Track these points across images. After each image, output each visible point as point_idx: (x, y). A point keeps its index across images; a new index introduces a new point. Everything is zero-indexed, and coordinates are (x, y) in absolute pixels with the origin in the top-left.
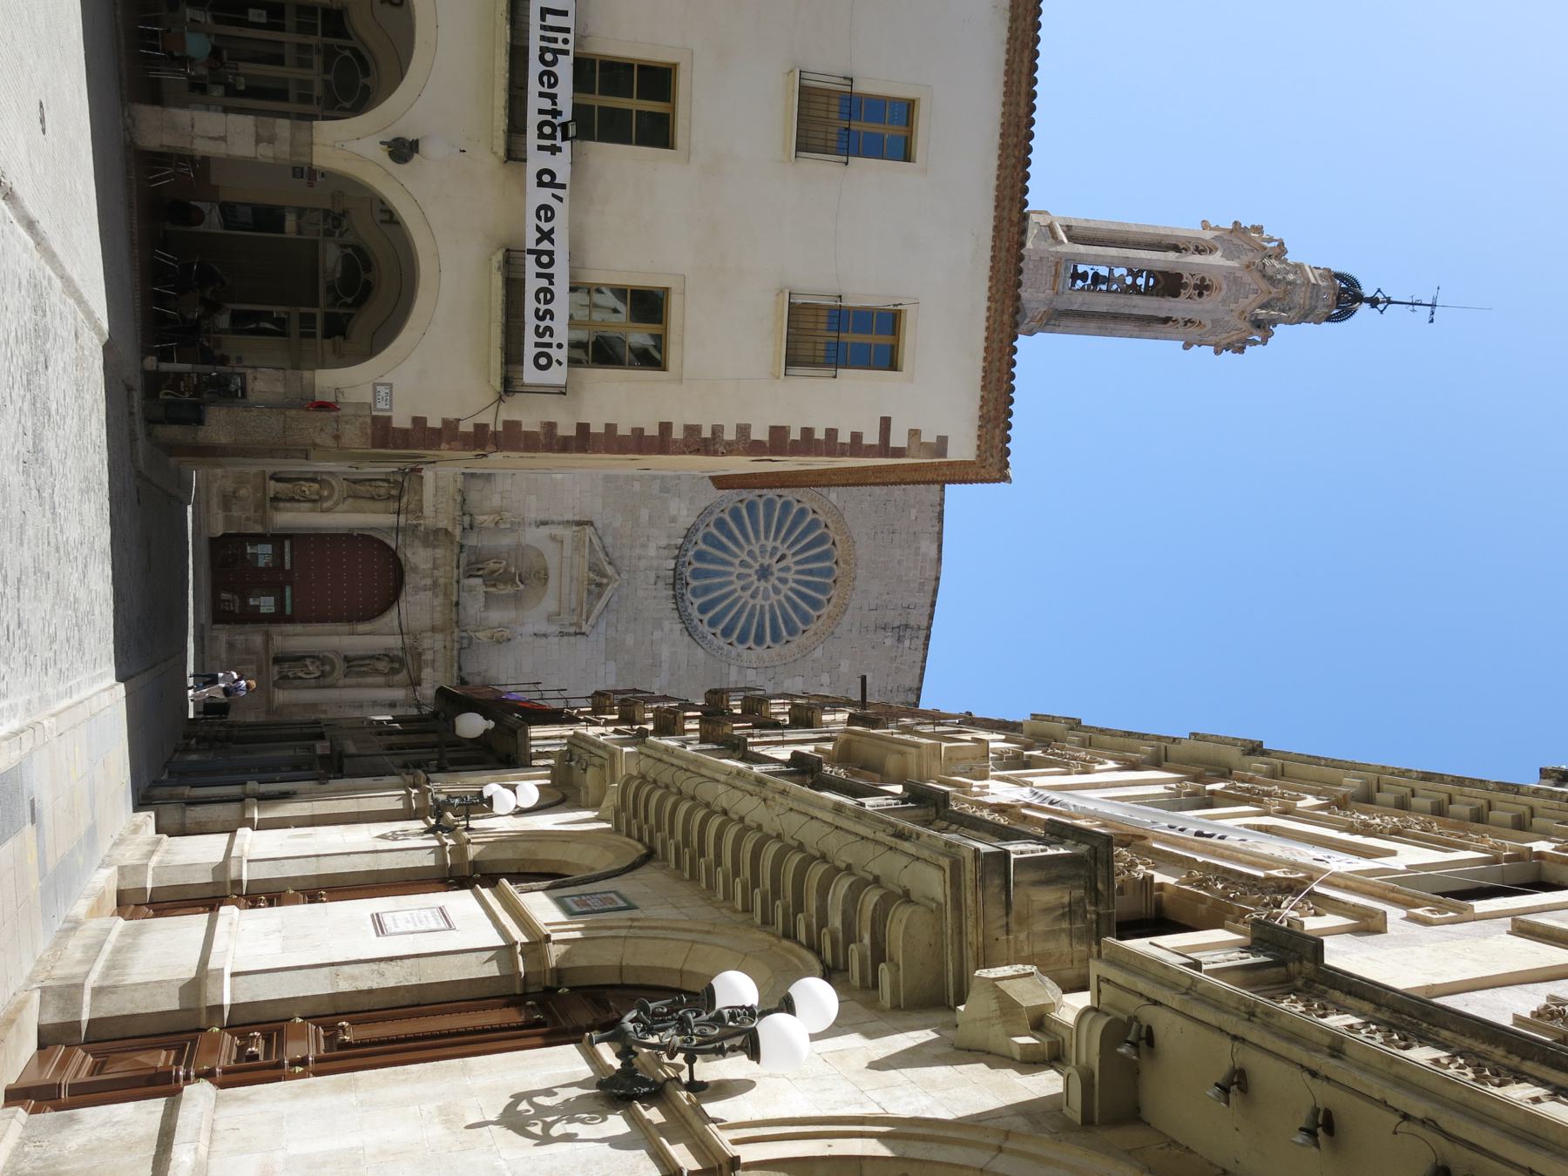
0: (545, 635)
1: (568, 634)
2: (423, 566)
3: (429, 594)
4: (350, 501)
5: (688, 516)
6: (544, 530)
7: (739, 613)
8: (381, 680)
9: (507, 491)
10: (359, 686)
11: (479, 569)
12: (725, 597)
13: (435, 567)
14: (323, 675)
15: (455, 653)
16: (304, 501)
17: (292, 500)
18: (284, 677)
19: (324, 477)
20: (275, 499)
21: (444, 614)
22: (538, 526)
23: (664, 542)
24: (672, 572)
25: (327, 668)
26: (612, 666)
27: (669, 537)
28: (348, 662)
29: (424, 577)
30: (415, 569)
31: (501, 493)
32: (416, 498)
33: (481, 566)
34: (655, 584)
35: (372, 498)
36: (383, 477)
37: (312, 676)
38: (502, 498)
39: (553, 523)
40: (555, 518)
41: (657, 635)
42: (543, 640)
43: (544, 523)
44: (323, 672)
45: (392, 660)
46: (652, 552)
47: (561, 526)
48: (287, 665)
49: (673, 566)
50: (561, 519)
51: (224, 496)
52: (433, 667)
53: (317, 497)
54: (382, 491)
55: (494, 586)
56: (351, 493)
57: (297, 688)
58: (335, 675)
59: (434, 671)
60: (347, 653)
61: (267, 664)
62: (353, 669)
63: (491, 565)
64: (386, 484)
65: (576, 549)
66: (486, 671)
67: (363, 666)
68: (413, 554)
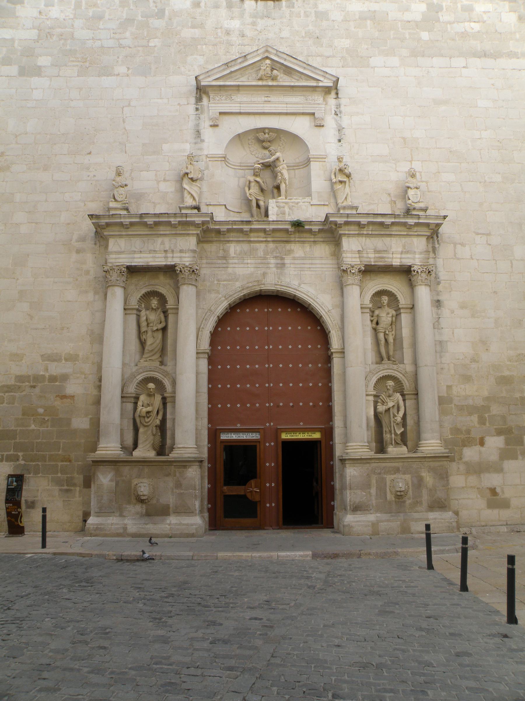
0: (340, 130)
1: (338, 106)
6: (207, 133)
8: (405, 318)
9: (156, 175)
10: (414, 345)
11: (258, 206)
14: (400, 388)
16: (165, 415)
17: (162, 427)
18: (403, 439)
20: (161, 450)
22: (203, 141)
26: (377, 61)
33: (254, 204)
35: (164, 330)
37: (401, 403)
38: (165, 180)
39: (198, 125)
40: (191, 124)
41: (336, 16)
43: (198, 133)
46: (235, 24)
48: (387, 437)
50: (192, 118)
51: (148, 514)
53: (158, 399)
55: (278, 188)
56: (158, 355)
62: (391, 353)
64: (143, 313)
66: (389, 194)
67: (386, 340)
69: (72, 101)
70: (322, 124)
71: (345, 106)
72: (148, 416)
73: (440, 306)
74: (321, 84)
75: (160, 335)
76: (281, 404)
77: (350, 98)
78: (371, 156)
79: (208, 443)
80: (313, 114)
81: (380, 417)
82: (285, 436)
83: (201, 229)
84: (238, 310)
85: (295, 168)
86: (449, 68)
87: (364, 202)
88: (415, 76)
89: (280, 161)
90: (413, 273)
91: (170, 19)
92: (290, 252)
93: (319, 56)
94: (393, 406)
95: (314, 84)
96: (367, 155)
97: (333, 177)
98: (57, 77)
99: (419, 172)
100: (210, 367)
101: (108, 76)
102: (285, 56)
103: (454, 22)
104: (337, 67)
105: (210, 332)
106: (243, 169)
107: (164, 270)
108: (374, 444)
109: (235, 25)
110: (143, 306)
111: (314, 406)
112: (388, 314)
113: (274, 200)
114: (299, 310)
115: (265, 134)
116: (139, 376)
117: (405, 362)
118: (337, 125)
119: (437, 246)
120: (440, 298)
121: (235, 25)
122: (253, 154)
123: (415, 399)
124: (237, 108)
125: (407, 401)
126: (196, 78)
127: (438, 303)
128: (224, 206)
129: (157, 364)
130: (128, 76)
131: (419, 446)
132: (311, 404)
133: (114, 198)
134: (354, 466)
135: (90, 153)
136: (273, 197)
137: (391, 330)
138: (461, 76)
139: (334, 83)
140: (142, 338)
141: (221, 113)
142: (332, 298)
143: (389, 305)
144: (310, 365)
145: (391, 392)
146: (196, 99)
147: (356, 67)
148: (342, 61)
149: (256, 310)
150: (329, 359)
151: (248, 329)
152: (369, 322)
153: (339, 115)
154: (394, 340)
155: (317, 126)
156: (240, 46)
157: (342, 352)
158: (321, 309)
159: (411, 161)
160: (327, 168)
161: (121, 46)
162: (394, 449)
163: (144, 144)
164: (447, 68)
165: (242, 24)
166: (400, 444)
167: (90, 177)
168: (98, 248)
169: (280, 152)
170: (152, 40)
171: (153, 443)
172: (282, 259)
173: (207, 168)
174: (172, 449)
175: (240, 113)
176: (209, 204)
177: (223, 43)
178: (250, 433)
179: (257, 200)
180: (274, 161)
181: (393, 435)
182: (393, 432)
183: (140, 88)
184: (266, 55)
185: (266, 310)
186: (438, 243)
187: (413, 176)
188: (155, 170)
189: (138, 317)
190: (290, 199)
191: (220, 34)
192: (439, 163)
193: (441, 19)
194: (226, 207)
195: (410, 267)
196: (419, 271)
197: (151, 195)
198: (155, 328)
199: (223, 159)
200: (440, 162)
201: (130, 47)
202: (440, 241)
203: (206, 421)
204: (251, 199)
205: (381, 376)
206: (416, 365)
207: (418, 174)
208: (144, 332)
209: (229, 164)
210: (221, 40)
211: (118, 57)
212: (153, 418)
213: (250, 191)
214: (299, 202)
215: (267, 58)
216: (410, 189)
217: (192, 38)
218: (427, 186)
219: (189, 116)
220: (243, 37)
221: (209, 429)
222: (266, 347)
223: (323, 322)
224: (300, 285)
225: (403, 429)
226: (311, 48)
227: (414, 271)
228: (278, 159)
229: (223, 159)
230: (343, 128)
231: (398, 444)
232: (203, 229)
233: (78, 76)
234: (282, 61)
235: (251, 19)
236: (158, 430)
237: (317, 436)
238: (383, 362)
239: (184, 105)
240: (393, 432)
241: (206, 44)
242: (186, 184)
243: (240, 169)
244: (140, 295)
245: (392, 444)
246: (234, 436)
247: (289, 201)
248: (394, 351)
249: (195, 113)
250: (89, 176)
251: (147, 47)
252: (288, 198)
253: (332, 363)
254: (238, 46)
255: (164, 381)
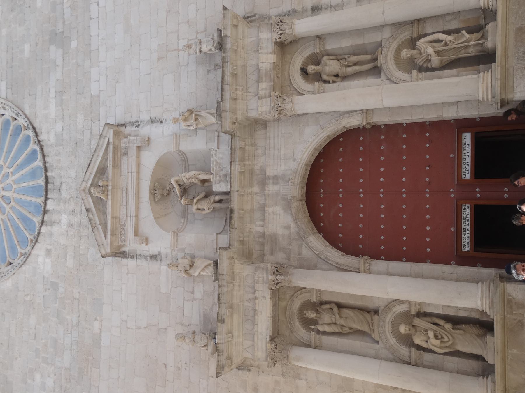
0: (152, 121)
1: (132, 124)
2: (279, 209)
3: (269, 172)
4: (371, 305)
5: (38, 256)
6: (152, 249)
7: (9, 152)
8: (331, 46)
9: (187, 300)
10: (360, 32)
11: (220, 201)
12: (21, 167)
13: (262, 208)
14: (412, 43)
15: (228, 95)
19: (404, 351)
21: (254, 145)
22: (159, 254)
23: (56, 229)
24: (49, 196)
25: (405, 53)
27: (51, 234)
28: (376, 67)
29: (277, 194)
30: (287, 205)
31: (194, 299)
32: (283, 304)
33: (217, 205)
34: (61, 183)
35: (340, 306)
36: (324, 338)
38: (193, 292)
39: (146, 257)
40: (144, 263)
42: (153, 116)
43: (153, 257)
44: (414, 47)
45: (318, 77)
47: (139, 253)
48: (472, 52)
49: (49, 202)
50: (139, 261)
52: (259, 70)
53: (417, 322)
54: (326, 318)
55: (204, 181)
56: (368, 316)
57: (455, 14)
58: (395, 44)
59: (258, 65)
60: (377, 81)
61: (506, 49)
62: (369, 57)
63: (205, 205)
64: (321, 328)
65: (123, 226)
67: (355, 64)
68: (288, 227)
69: (119, 377)
70: (147, 139)
71: (131, 117)
72: (440, 337)
73: (318, 7)
74: (111, 140)
75: (345, 311)
76: (427, 179)
77: (125, 113)
78: (174, 91)
79: (477, 266)
80: (139, 147)
81: (447, 63)
82: (467, 175)
83: (236, 260)
84: (322, 224)
85: (187, 165)
86: (99, 19)
87: (216, 96)
88: (106, 51)
89: (179, 180)
90: (283, 39)
91: (59, 277)
92: (263, 171)
93: (90, 142)
94: (433, 47)
95: (111, 147)
96: (173, 95)
97: (192, 128)
98: (99, 389)
99: (188, 42)
100: (382, 258)
101: (101, 340)
102: (88, 173)
103: (64, 18)
104: (100, 125)
105: (342, 255)
106: (188, 216)
107: (277, 301)
108: (482, 66)
109: (66, 218)
110: (313, 327)
111: (430, 141)
112: (326, 65)
113: (214, 185)
114: (322, 161)
115: (156, 193)
116: (391, 340)
117: (379, 40)
118: (148, 125)
119: (257, 17)
120: (310, 7)
121: (66, 218)
122: (174, 205)
123: (425, 22)
124: (132, 219)
125: (427, 32)
126: (103, 257)
127: (316, 9)
128: (219, 235)
129: (376, 317)
130: (101, 321)
131: (487, 8)
132: (428, 145)
133: (205, 346)
134: (513, 87)
135: (165, 365)
136: (211, 186)
137: (344, 59)
138: (105, 7)
139: (110, 128)
140: (348, 332)
141: (136, 235)
142: (308, 125)
143: (317, 63)
144: (382, 148)
145: (415, 52)
146: (123, 258)
147: (100, 108)
148: (94, 121)
149: (322, 205)
150: (376, 128)
151: (341, 215)
152: (335, 84)
153: (139, 123)
154: (354, 55)
155: (149, 144)
156: (82, 215)
157: (367, 112)
158: (319, 137)
159: (179, 51)
160: (185, 134)
161: (78, 325)
162: (489, 39)
163: (160, 311)
164: (99, 21)
165: (65, 212)
166: (484, 33)
167: (186, 367)
168: (254, 368)
169: (170, 179)
170: (74, 296)
171: (476, 335)
172: (269, 178)
173: (183, 250)
174: (483, 313)
175: (137, 217)
176: (215, 250)
177: (79, 230)
178: (463, 216)
179: (215, 202)
180: (180, 186)
181: (471, 43)
182: (465, 44)
183: (112, 310)
184: (87, 191)
185: (322, 195)
186: (254, 16)
187: (189, 47)
188: (184, 302)
189: (325, 333)
190: (213, 169)
191: (72, 233)
192: (180, 22)
193: (61, 30)
194: (220, 233)
195: (276, 43)
196: (281, 32)
197: (205, 307)
198: (337, 316)
199: (176, 234)
200: (178, 21)
201: (79, 316)
202: (253, 14)
203: (446, 268)
204: (213, 208)
205: (394, 66)
206: (383, 26)
207: (190, 43)
208: (342, 328)
209: (181, 228)
210: (76, 232)
211: (87, 328)
212: (442, 331)
213: (205, 209)
214: (216, 161)
215: (89, 190)
216: (202, 50)
217: (74, 258)
218: (201, 32)
219: (138, 265)
220: (74, 212)
221: (458, 264)
222: (361, 195)
223: (334, 134)
224: (295, 160)
225: (464, 32)
226: (84, 150)
227: (280, 38)
228: (177, 182)
229: (176, 234)
230: (150, 118)
231: (483, 35)
232: (236, 258)
233: (99, 368)
234: (92, 176)
235: (61, 204)
236: (459, 326)
237: (467, 138)
238: (379, 65)
239: (128, 269)
240: (465, 44)
241: (80, 246)
242: (195, 272)
243: (187, 218)
244: (302, 329)
245: (482, 44)
246: (467, 236)
247: (214, 171)
248: (367, 54)
249: (136, 259)
250: (186, 369)
251: (79, 301)
252: (212, 172)
253: (379, 124)
254: (82, 217)
255: (397, 312)
